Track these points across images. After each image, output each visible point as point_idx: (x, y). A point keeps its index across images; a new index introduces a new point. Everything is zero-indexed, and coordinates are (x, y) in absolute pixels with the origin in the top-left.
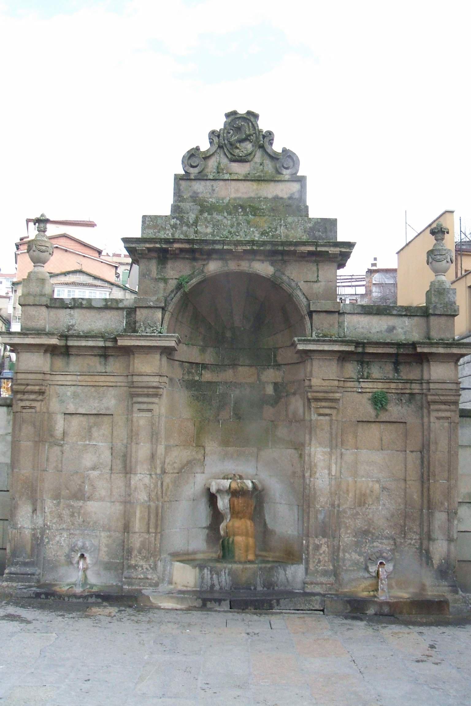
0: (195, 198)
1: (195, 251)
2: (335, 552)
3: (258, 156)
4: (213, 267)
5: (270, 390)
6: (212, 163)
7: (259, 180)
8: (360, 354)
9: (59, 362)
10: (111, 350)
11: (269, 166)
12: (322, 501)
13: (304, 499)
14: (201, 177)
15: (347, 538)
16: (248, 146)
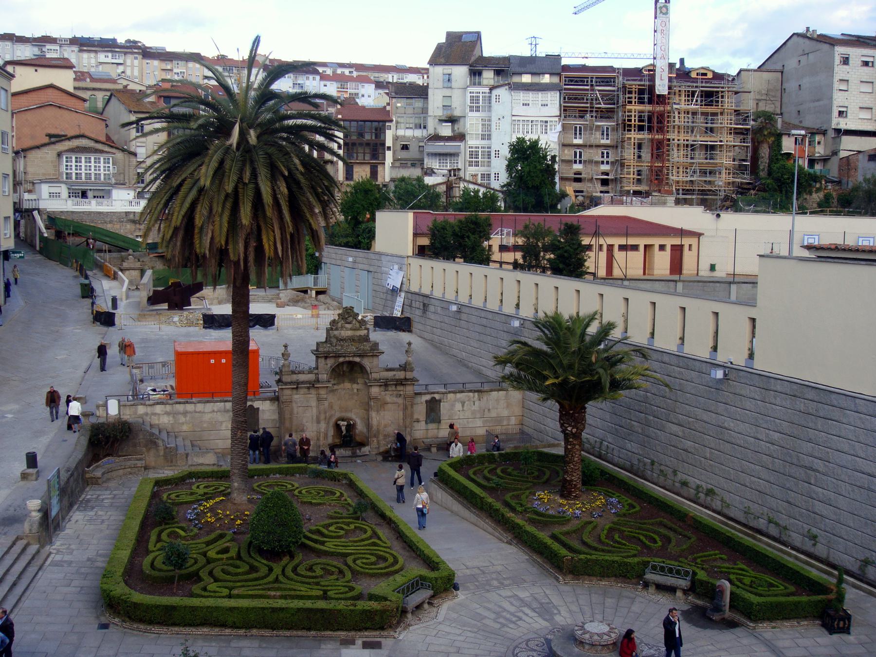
0: (335, 337)
1: (337, 356)
2: (378, 443)
3: (354, 321)
4: (341, 360)
5: (355, 391)
6: (340, 325)
7: (355, 330)
8: (385, 384)
9: (295, 391)
10: (312, 385)
11: (358, 325)
12: (375, 428)
13: (368, 426)
14: (337, 329)
15: (381, 437)
16: (351, 318)
